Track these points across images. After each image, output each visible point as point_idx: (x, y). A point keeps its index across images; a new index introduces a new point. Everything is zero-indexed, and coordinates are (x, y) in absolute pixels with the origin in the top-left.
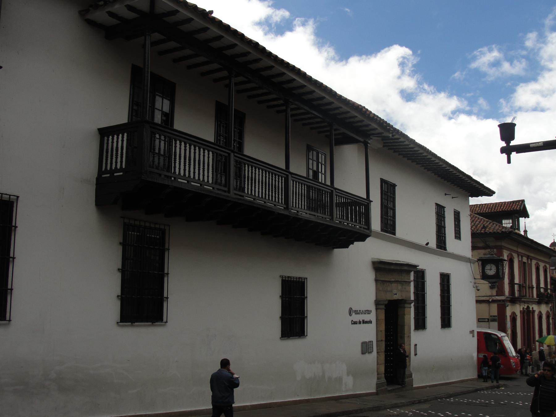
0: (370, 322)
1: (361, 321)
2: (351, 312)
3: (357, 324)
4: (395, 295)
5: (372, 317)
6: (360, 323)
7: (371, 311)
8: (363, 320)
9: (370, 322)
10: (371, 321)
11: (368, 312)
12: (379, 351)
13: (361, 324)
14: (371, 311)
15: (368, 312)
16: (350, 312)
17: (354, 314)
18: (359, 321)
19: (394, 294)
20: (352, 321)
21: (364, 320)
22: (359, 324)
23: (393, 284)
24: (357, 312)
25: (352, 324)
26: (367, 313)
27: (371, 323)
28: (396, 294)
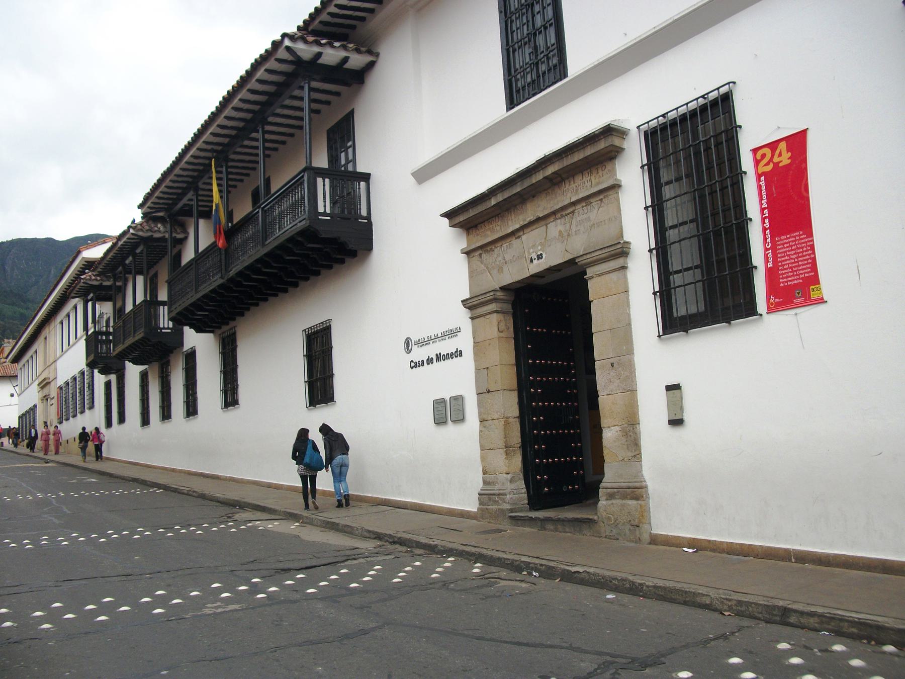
0: (459, 353)
1: (432, 359)
2: (408, 345)
3: (423, 365)
4: (535, 262)
5: (465, 342)
6: (430, 361)
7: (459, 330)
8: (437, 354)
9: (459, 353)
10: (461, 351)
11: (453, 333)
12: (485, 417)
13: (432, 363)
14: (459, 330)
15: (453, 333)
16: (408, 347)
17: (415, 348)
18: (428, 359)
19: (531, 261)
20: (412, 361)
21: (440, 354)
22: (428, 364)
23: (524, 237)
24: (421, 343)
25: (412, 368)
26: (447, 337)
27: (461, 355)
28: (540, 257)
